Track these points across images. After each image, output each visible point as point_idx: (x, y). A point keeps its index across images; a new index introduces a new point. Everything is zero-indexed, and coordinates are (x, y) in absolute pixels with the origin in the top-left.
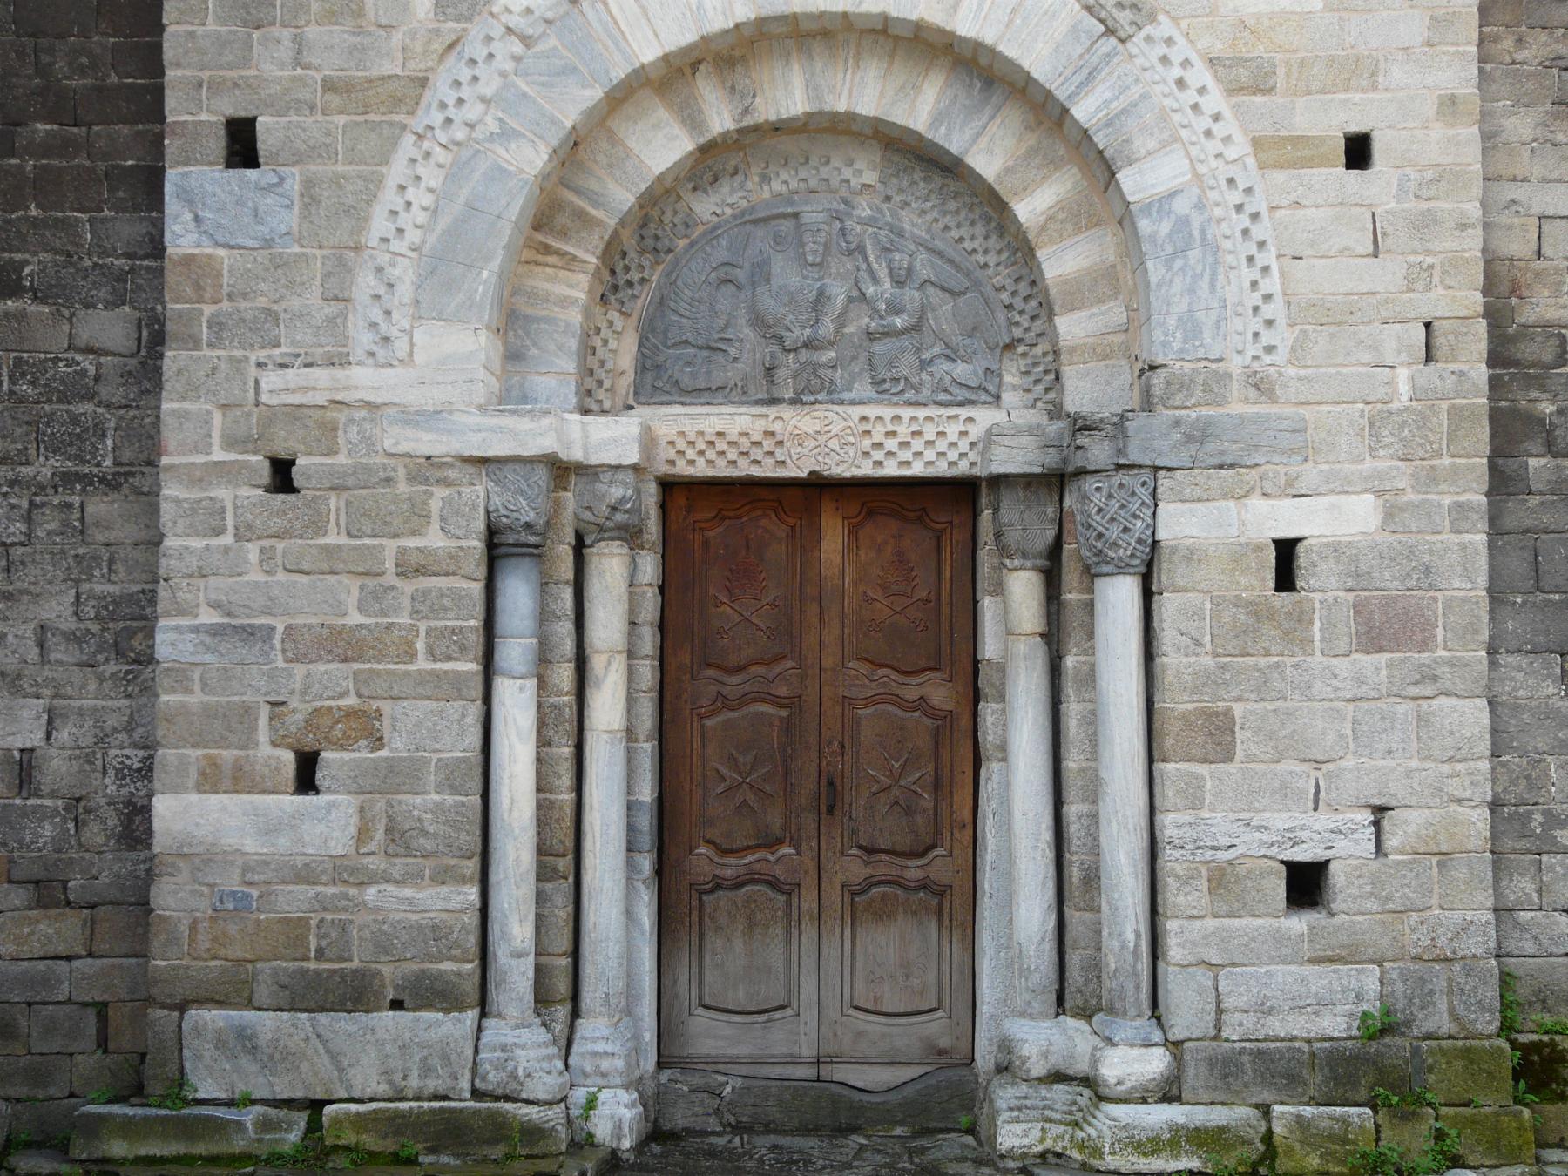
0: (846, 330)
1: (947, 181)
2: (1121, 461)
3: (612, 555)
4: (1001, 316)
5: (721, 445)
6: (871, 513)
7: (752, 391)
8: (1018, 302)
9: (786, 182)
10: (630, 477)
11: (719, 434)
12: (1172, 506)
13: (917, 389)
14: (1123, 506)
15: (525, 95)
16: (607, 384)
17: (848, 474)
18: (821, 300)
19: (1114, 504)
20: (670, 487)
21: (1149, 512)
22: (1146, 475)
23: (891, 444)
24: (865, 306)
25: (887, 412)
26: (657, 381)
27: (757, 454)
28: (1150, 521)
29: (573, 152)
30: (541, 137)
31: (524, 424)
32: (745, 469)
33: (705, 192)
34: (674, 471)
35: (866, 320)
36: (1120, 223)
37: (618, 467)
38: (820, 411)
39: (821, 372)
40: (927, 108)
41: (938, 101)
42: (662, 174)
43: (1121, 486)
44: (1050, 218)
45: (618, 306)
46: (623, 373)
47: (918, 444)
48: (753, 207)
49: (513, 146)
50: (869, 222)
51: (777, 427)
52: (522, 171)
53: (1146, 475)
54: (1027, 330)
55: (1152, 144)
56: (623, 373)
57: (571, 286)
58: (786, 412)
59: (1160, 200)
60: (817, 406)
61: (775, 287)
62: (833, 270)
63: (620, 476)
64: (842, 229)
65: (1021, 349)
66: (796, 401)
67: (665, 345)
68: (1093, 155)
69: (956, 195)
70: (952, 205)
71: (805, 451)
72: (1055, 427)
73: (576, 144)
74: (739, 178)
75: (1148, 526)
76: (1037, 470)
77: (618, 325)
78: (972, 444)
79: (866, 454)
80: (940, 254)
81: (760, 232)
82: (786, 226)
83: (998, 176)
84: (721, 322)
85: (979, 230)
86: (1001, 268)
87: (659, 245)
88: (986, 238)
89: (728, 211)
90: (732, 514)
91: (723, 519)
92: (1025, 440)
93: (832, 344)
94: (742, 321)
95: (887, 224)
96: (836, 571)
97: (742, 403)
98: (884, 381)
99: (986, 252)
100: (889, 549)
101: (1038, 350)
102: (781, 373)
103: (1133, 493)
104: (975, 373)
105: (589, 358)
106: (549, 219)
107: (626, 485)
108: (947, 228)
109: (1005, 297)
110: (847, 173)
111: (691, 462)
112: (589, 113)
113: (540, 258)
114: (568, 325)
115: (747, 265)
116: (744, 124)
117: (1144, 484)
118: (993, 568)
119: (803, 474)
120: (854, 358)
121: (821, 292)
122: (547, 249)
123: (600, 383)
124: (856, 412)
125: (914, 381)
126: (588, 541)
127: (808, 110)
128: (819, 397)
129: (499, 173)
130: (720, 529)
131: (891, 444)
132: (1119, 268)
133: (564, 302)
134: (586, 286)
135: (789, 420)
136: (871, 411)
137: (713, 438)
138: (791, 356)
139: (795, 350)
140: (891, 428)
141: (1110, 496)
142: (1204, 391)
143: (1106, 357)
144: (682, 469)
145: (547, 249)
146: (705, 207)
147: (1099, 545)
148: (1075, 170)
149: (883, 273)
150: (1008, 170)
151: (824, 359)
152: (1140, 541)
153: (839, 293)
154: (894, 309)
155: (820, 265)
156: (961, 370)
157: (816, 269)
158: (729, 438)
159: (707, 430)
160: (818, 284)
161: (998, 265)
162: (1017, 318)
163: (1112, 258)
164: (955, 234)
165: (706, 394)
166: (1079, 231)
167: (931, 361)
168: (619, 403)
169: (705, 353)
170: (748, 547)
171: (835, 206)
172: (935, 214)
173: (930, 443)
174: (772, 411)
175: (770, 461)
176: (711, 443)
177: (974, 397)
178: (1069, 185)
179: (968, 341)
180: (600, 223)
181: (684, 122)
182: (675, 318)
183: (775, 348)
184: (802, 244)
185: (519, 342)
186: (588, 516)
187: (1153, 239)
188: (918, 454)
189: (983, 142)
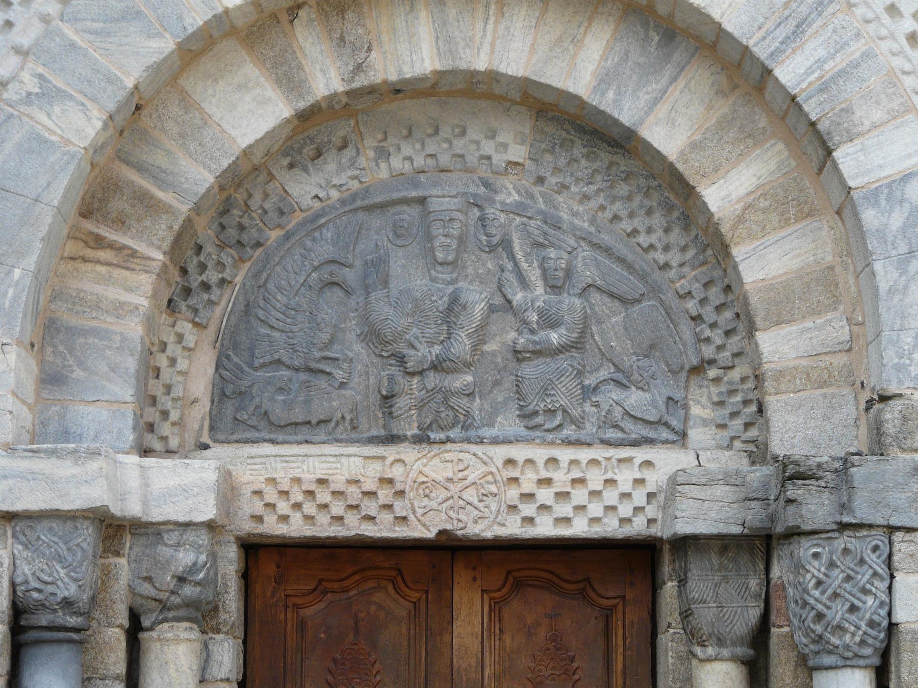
0: (487, 348)
1: (616, 158)
2: (846, 519)
3: (178, 641)
4: (686, 330)
5: (323, 497)
6: (519, 585)
7: (364, 424)
8: (708, 313)
9: (409, 159)
10: (204, 538)
11: (322, 482)
13: (578, 423)
14: (848, 578)
15: (73, 45)
16: (174, 416)
17: (489, 535)
18: (454, 306)
19: (838, 576)
20: (254, 550)
21: (883, 586)
22: (878, 538)
23: (545, 495)
24: (510, 317)
25: (540, 454)
26: (238, 413)
27: (370, 506)
28: (884, 597)
29: (134, 119)
30: (94, 100)
31: (65, 469)
32: (354, 527)
33: (305, 170)
35: (513, 335)
36: (838, 213)
37: (188, 525)
38: (453, 452)
39: (453, 401)
40: (591, 67)
41: (604, 58)
42: (250, 147)
43: (846, 551)
44: (749, 206)
45: (190, 315)
46: (195, 401)
47: (579, 496)
48: (367, 190)
49: (57, 109)
50: (518, 210)
51: (396, 472)
52: (68, 142)
53: (878, 538)
54: (720, 348)
55: (878, 115)
56: (195, 401)
57: (129, 290)
58: (408, 452)
59: (889, 186)
60: (449, 446)
61: (394, 292)
62: (470, 271)
63: (190, 536)
64: (482, 219)
65: (712, 373)
66: (422, 439)
67: (251, 365)
68: (803, 128)
69: (628, 176)
70: (623, 189)
71: (433, 504)
72: (759, 474)
73: (138, 108)
74: (349, 152)
75: (882, 604)
76: (736, 530)
77: (190, 339)
78: (651, 496)
79: (513, 508)
80: (607, 251)
81: (376, 221)
82: (410, 213)
83: (682, 153)
84: (325, 337)
85: (658, 220)
86: (686, 269)
87: (245, 238)
88: (667, 230)
89: (335, 194)
90: (336, 586)
91: (325, 592)
92: (720, 491)
93: (468, 365)
94: (351, 336)
95: (541, 212)
96: (473, 661)
97: (350, 441)
98: (536, 413)
99: (666, 248)
100: (542, 633)
101: (735, 374)
102: (402, 403)
103: (862, 561)
104: (653, 403)
105: (152, 382)
106: (101, 203)
107: (198, 548)
108: (616, 218)
109: (691, 306)
110: (488, 147)
111: (284, 518)
112: (156, 70)
113: (89, 253)
114: (124, 339)
115: (358, 263)
116: (356, 85)
117: (875, 549)
118: (680, 658)
119: (431, 534)
120: (497, 383)
121: (454, 299)
122: (99, 242)
123: (165, 414)
124: (500, 453)
125: (575, 413)
126: (146, 622)
127: (438, 67)
128: (452, 434)
129: (38, 143)
130: (322, 605)
131: (545, 495)
132: (838, 269)
133: (120, 309)
134: (148, 289)
135: (413, 464)
136: (520, 453)
137: (313, 487)
138: (415, 380)
139: (420, 373)
140: (544, 474)
141: (832, 565)
143: (823, 384)
144: (272, 527)
145: (99, 242)
146: (305, 189)
147: (819, 628)
148: (780, 146)
149: (534, 275)
150: (694, 146)
151: (458, 384)
152: (872, 624)
153: (477, 299)
154: (550, 321)
155: (453, 264)
156: (635, 399)
157: (450, 268)
158: (333, 487)
159: (305, 476)
160: (451, 289)
161: (682, 265)
162: (708, 333)
163: (829, 258)
164: (626, 225)
165: (305, 429)
166: (786, 222)
167: (596, 389)
168: (190, 440)
169: (303, 376)
170: (357, 631)
171: (472, 189)
172: (601, 200)
174: (391, 452)
175: (386, 517)
176: (310, 493)
177: (652, 434)
178: (773, 166)
179: (644, 363)
180: (168, 209)
181: (278, 82)
182: (264, 330)
183: (394, 370)
184: (430, 238)
185: (59, 361)
186: (147, 589)
187: (881, 234)
188: (580, 508)
189: (662, 110)
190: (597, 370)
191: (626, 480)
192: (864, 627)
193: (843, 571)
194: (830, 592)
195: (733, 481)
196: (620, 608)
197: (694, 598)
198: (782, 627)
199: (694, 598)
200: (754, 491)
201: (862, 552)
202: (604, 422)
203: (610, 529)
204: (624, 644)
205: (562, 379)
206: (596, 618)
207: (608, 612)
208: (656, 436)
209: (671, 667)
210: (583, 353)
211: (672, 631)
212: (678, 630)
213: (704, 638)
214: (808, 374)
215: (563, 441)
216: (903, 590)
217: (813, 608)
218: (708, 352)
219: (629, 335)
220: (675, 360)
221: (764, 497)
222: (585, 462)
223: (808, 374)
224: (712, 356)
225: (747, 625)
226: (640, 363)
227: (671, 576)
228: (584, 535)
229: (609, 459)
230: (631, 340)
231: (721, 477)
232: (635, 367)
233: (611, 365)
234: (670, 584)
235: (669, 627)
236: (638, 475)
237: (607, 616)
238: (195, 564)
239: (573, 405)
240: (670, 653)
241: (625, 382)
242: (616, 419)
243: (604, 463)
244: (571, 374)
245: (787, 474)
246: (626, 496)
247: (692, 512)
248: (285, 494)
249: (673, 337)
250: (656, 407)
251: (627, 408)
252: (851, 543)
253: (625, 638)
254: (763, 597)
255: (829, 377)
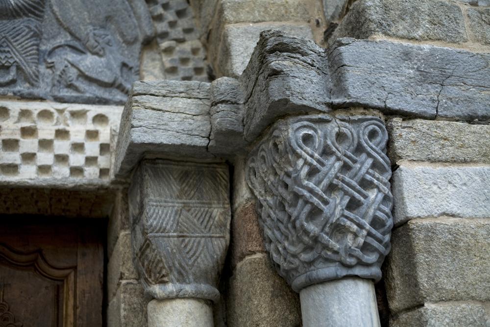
12: (418, 168)
14: (346, 167)
19: (333, 166)
21: (386, 177)
28: (386, 190)
43: (340, 136)
54: (172, 24)
65: (165, 44)
75: (386, 198)
78: (104, 148)
92: (181, 103)
101: (187, 46)
103: (359, 149)
104: (108, 66)
118: (133, 310)
125: (30, 69)
141: (326, 152)
142: (431, 22)
152: (376, 222)
156: (88, 62)
167: (51, 53)
173: (45, 144)
188: (29, 157)
190: (54, 37)
191: (78, 131)
192: (368, 227)
193: (338, 159)
194: (325, 182)
195: (195, 94)
196: (72, 277)
197: (151, 225)
198: (254, 253)
199: (151, 225)
200: (222, 94)
201: (359, 137)
202: (58, 81)
203: (59, 177)
204: (75, 314)
205: (18, 38)
206: (47, 288)
207: (59, 283)
208: (110, 97)
209: (123, 320)
210: (42, 22)
211: (124, 282)
212: (131, 281)
213: (164, 272)
214: (266, 8)
215: (15, 94)
216: (410, 180)
217: (307, 202)
218: (161, 27)
219: (87, 7)
220: (130, 31)
221: (233, 100)
222: (36, 113)
223: (266, 8)
224: (164, 29)
225: (212, 257)
226: (96, 32)
227: (124, 224)
228: (31, 182)
229: (61, 111)
230: (88, 12)
231: (182, 90)
232: (91, 34)
233: (68, 34)
234: (122, 233)
235: (121, 278)
236: (91, 127)
237: (58, 286)
239: (27, 63)
240: (123, 305)
241: (80, 47)
242: (70, 79)
243: (56, 115)
244: (27, 34)
245: (268, 48)
246: (78, 147)
247: (151, 122)
249: (128, 12)
250: (110, 70)
251: (82, 69)
252: (346, 127)
253: (75, 307)
254: (228, 227)
255: (286, 12)
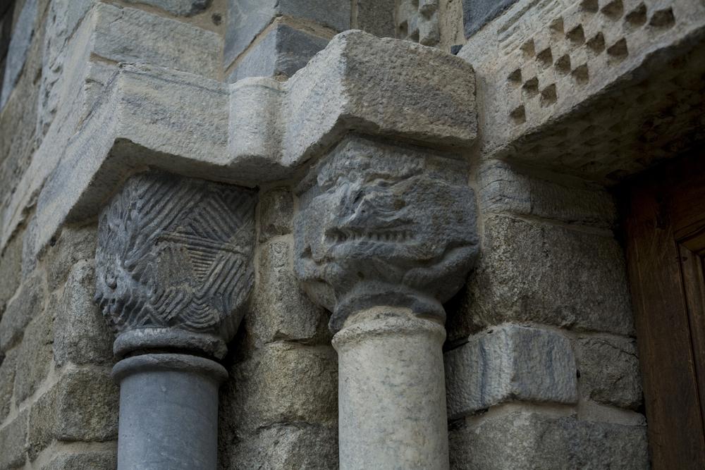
10: (353, 154)
34: (523, 128)
144: (540, 114)
238: (343, 202)
248: (545, 56)
